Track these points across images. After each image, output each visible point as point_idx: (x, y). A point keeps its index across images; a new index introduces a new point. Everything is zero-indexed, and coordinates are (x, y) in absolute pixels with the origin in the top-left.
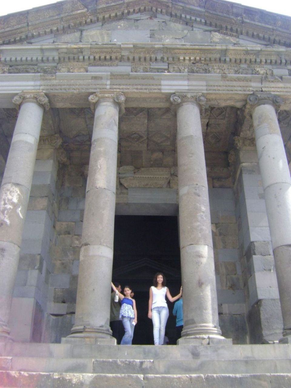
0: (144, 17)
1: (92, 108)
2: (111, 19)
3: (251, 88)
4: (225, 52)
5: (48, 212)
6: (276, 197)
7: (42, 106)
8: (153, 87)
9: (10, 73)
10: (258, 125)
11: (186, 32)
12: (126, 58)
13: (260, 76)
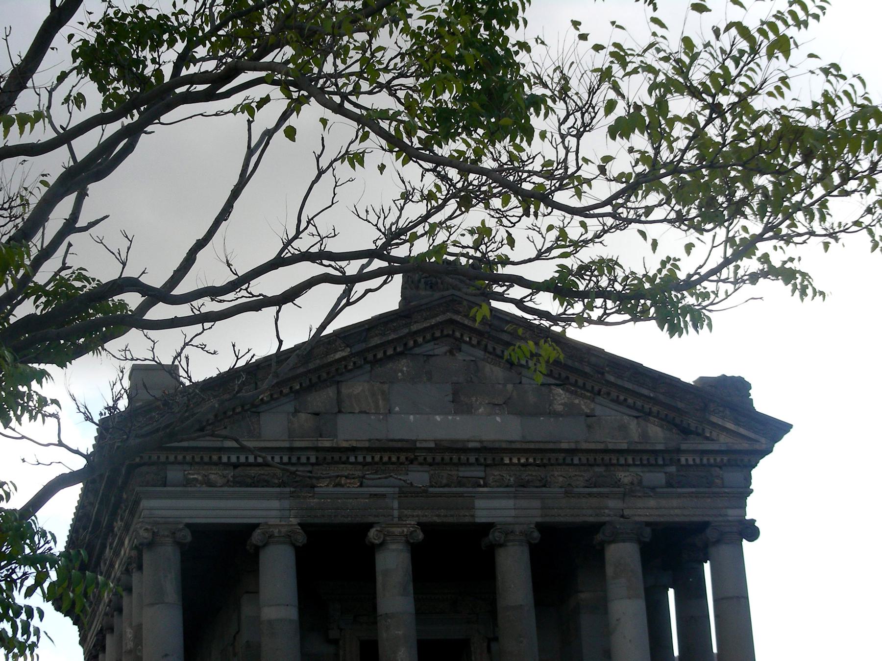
3: (606, 511)
11: (510, 387)
12: (421, 459)
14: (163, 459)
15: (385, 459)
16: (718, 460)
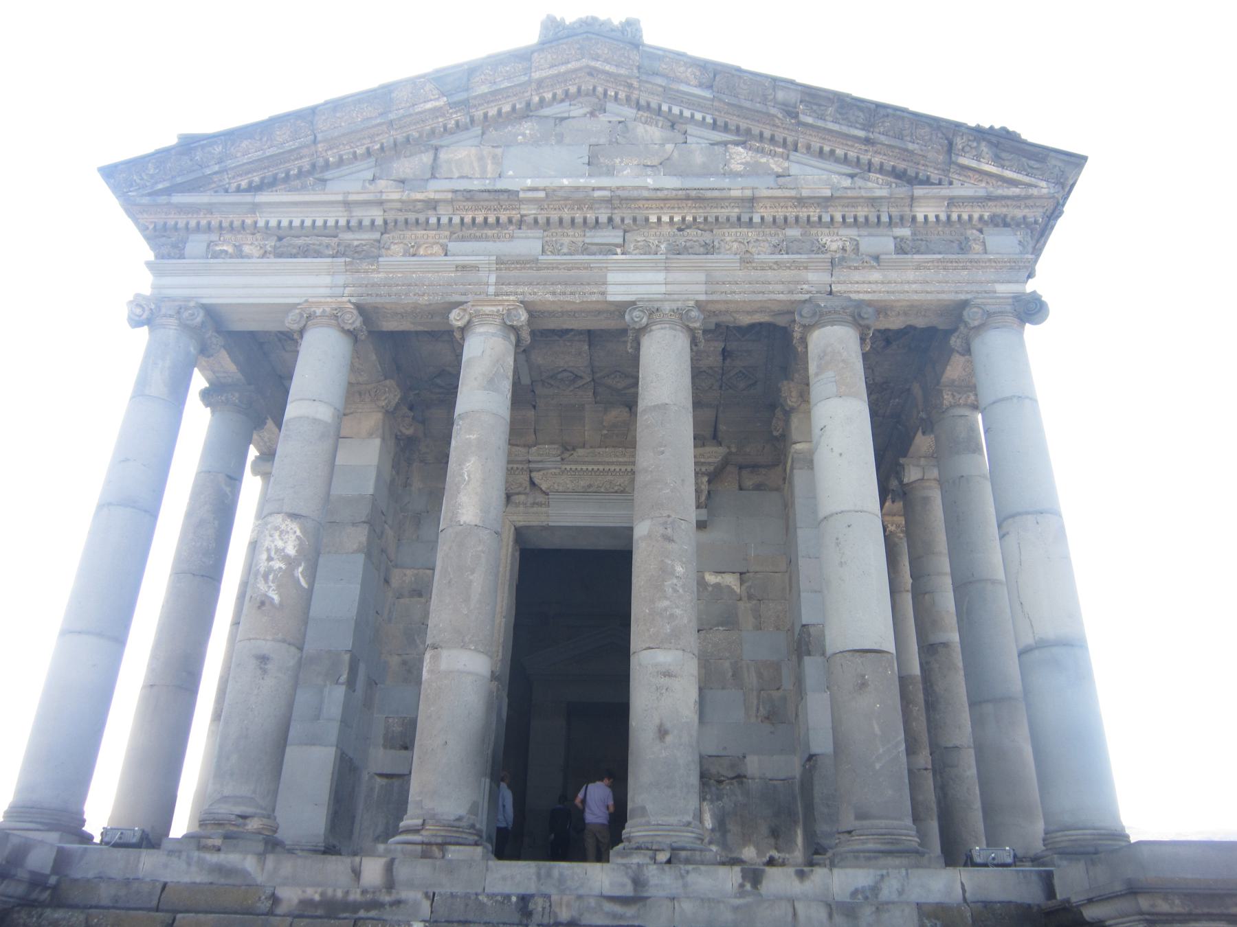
0: (577, 111)
1: (457, 335)
2: (502, 119)
3: (805, 287)
5: (369, 555)
6: (838, 544)
7: (352, 334)
8: (588, 289)
9: (280, 256)
10: (817, 374)
11: (669, 147)
13: (828, 256)
16: (976, 216)
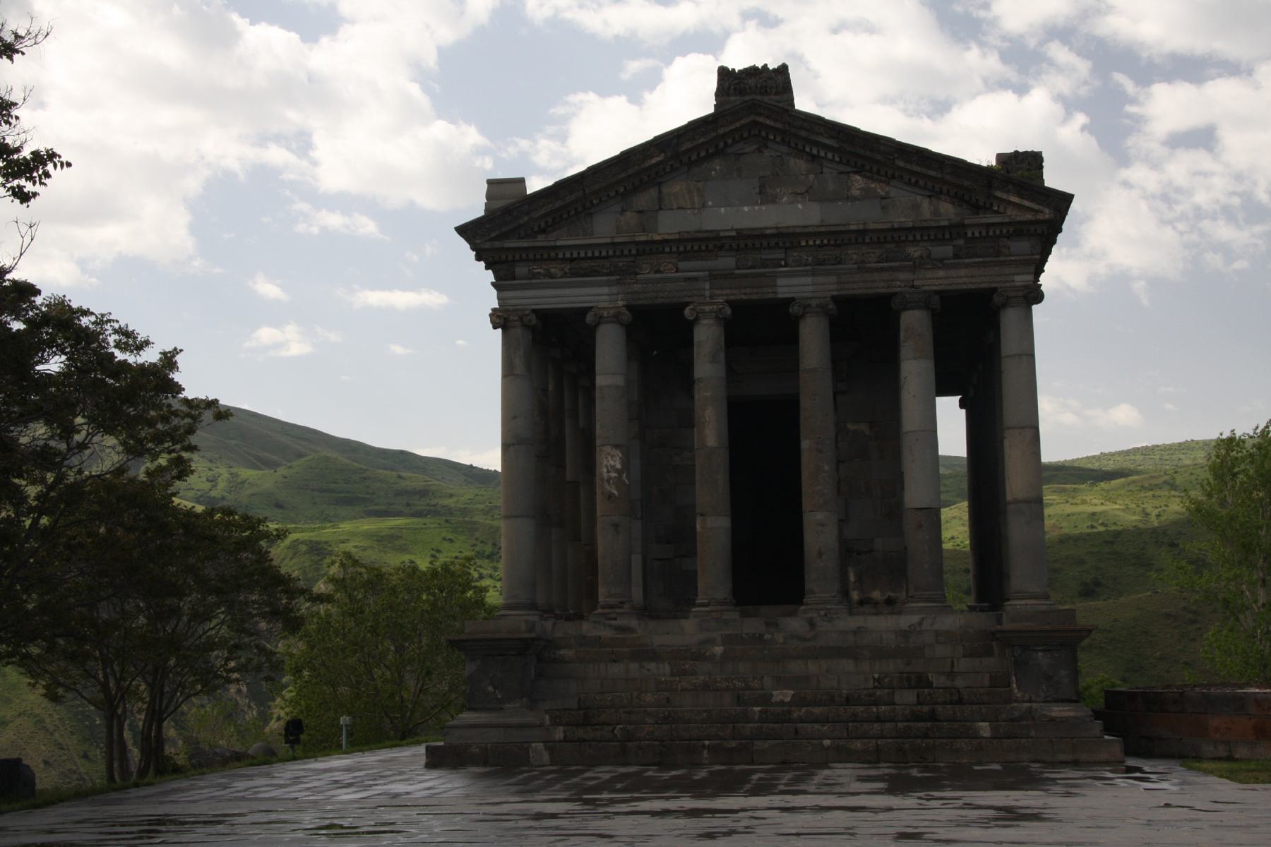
0: (749, 149)
4: (863, 232)
9: (574, 274)
11: (811, 177)
14: (510, 258)
15: (696, 248)
